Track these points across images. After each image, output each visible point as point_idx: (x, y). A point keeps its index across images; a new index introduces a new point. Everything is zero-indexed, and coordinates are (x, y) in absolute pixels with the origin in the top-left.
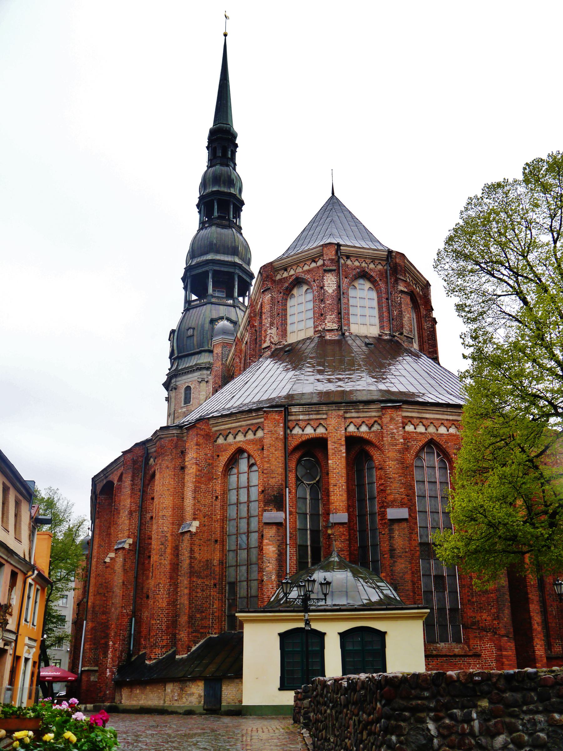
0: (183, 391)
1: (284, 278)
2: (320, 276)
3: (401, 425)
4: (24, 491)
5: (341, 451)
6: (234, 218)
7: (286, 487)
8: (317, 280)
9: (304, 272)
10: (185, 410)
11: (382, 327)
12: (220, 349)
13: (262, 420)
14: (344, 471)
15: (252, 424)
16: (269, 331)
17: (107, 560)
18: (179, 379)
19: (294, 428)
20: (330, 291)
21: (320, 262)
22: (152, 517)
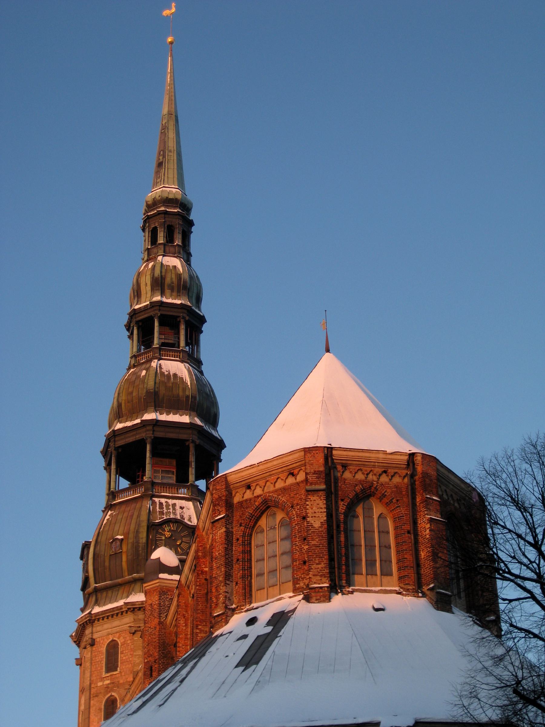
0: (104, 649)
1: (246, 500)
2: (301, 499)
6: (187, 344)
8: (297, 504)
9: (276, 491)
10: (108, 682)
16: (223, 589)
18: (99, 628)
20: (317, 524)
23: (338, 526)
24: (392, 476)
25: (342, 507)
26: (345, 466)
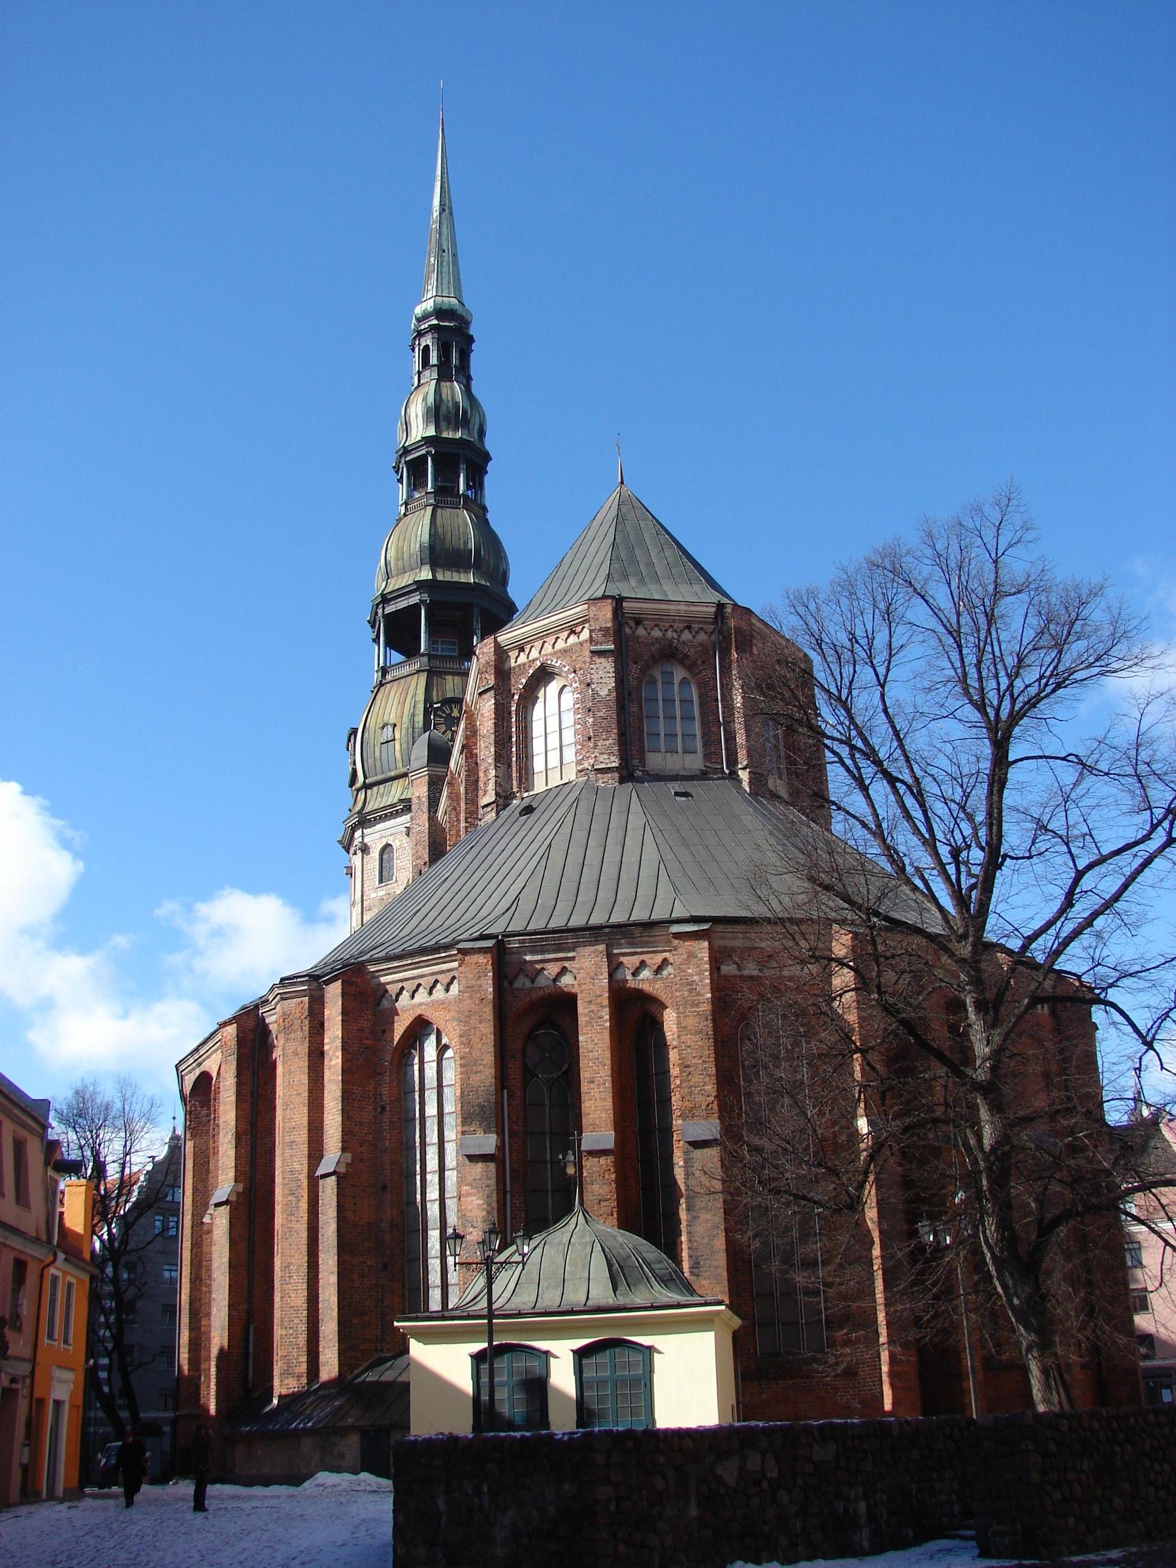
2: (584, 662)
4: (30, 1122)
6: (468, 487)
10: (383, 893)
12: (426, 789)
13: (455, 964)
14: (608, 1054)
15: (442, 972)
19: (516, 976)
20: (604, 692)
23: (630, 694)
24: (697, 633)
26: (638, 622)
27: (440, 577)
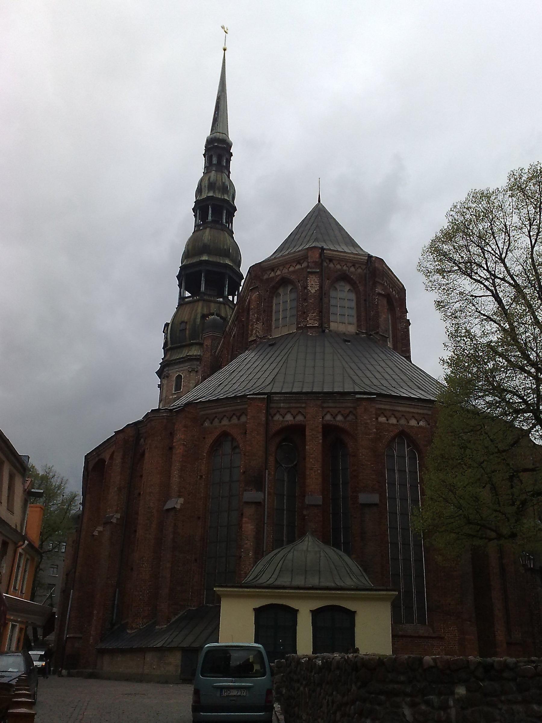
1: (271, 278)
3: (374, 416)
4: (18, 465)
5: (318, 437)
7: (266, 469)
11: (359, 326)
13: (246, 406)
17: (96, 533)
18: (172, 368)
19: (275, 414)
20: (313, 291)
21: (305, 265)
22: (140, 494)
25: (327, 282)
26: (331, 260)
27: (211, 259)
